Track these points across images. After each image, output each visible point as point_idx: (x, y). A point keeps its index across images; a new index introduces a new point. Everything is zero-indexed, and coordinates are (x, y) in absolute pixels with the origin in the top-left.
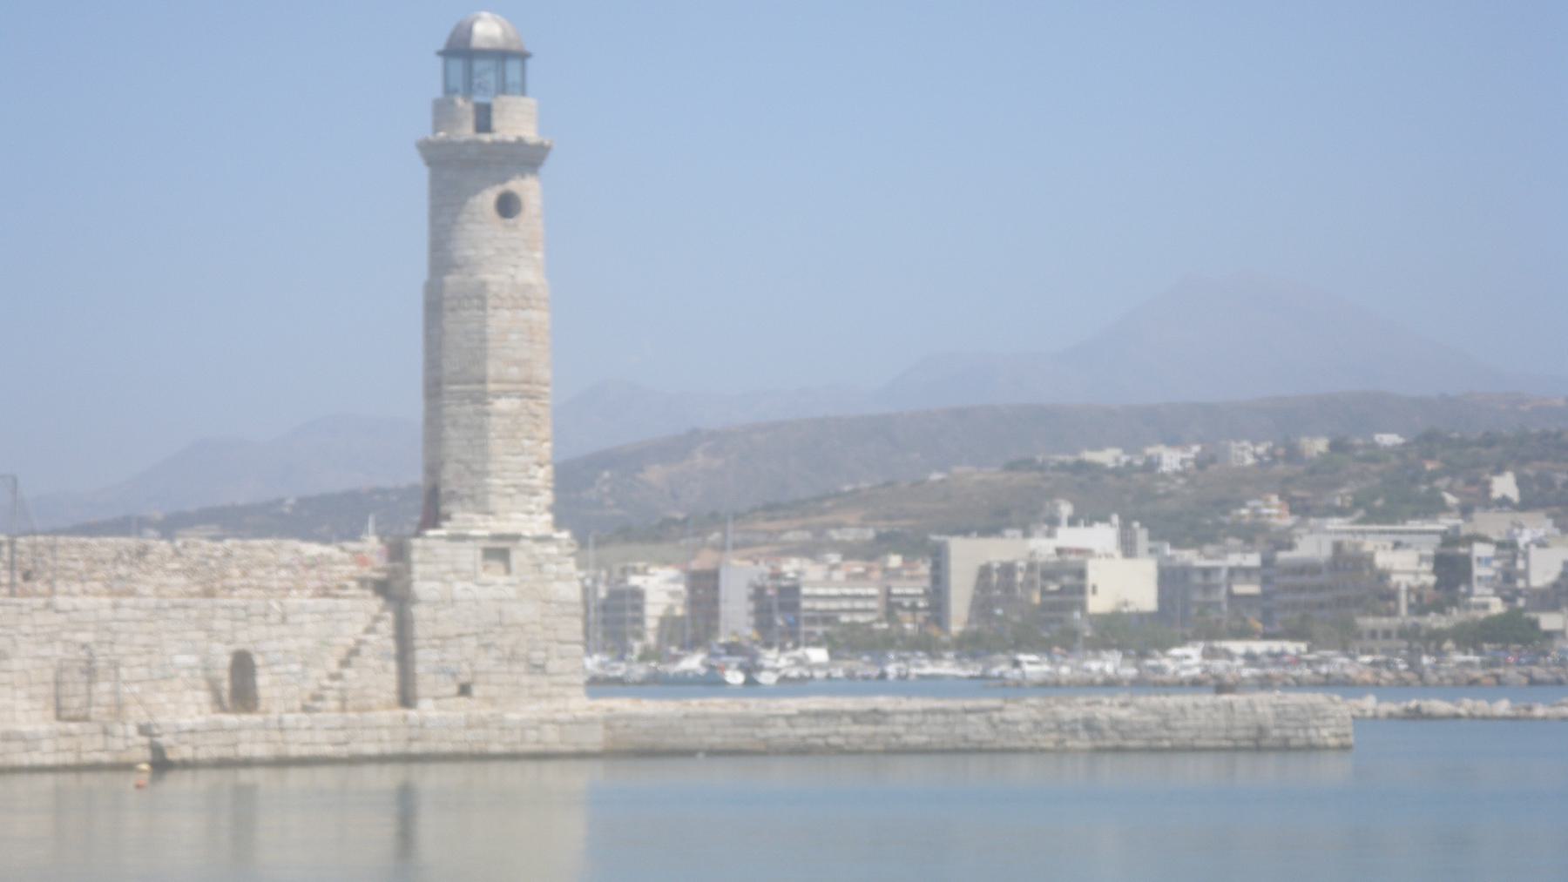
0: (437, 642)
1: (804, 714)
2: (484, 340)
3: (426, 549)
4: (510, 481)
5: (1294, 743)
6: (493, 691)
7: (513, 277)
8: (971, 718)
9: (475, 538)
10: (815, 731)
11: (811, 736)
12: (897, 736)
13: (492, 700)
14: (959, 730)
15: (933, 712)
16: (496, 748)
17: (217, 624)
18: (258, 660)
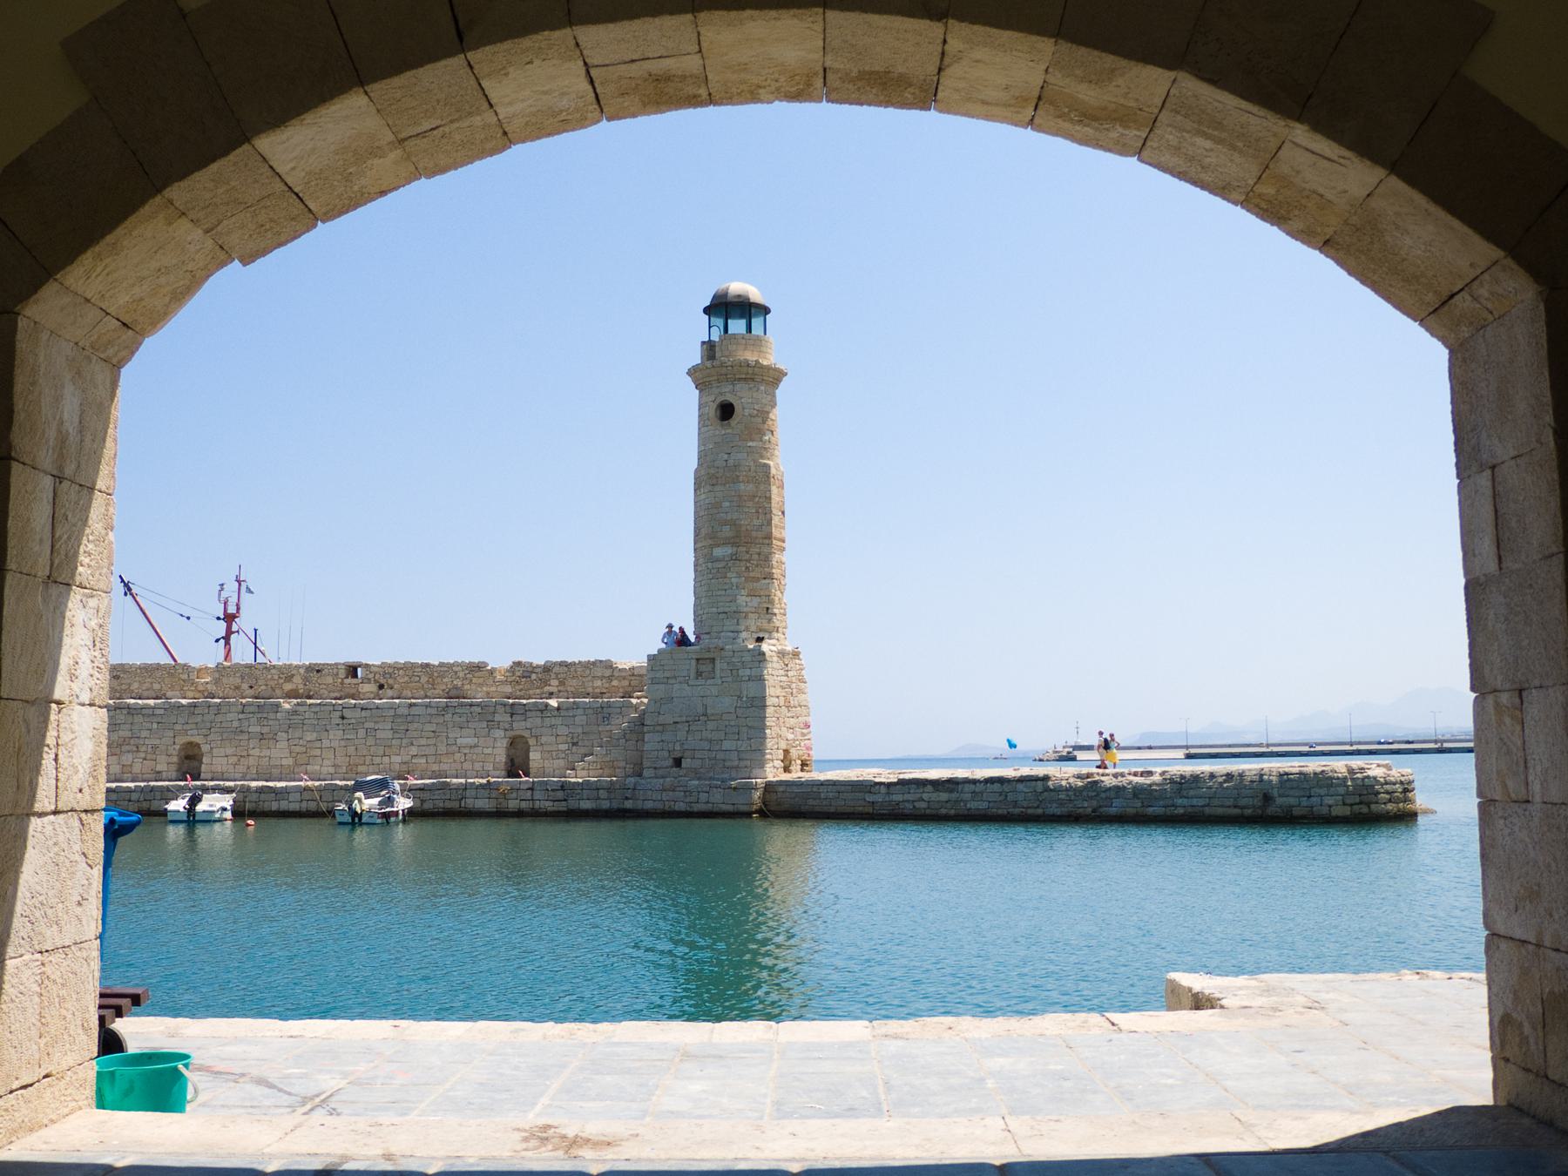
0: (660, 728)
4: (721, 610)
5: (1296, 812)
6: (697, 763)
7: (726, 461)
10: (907, 797)
14: (1011, 797)
17: (497, 718)
18: (532, 742)
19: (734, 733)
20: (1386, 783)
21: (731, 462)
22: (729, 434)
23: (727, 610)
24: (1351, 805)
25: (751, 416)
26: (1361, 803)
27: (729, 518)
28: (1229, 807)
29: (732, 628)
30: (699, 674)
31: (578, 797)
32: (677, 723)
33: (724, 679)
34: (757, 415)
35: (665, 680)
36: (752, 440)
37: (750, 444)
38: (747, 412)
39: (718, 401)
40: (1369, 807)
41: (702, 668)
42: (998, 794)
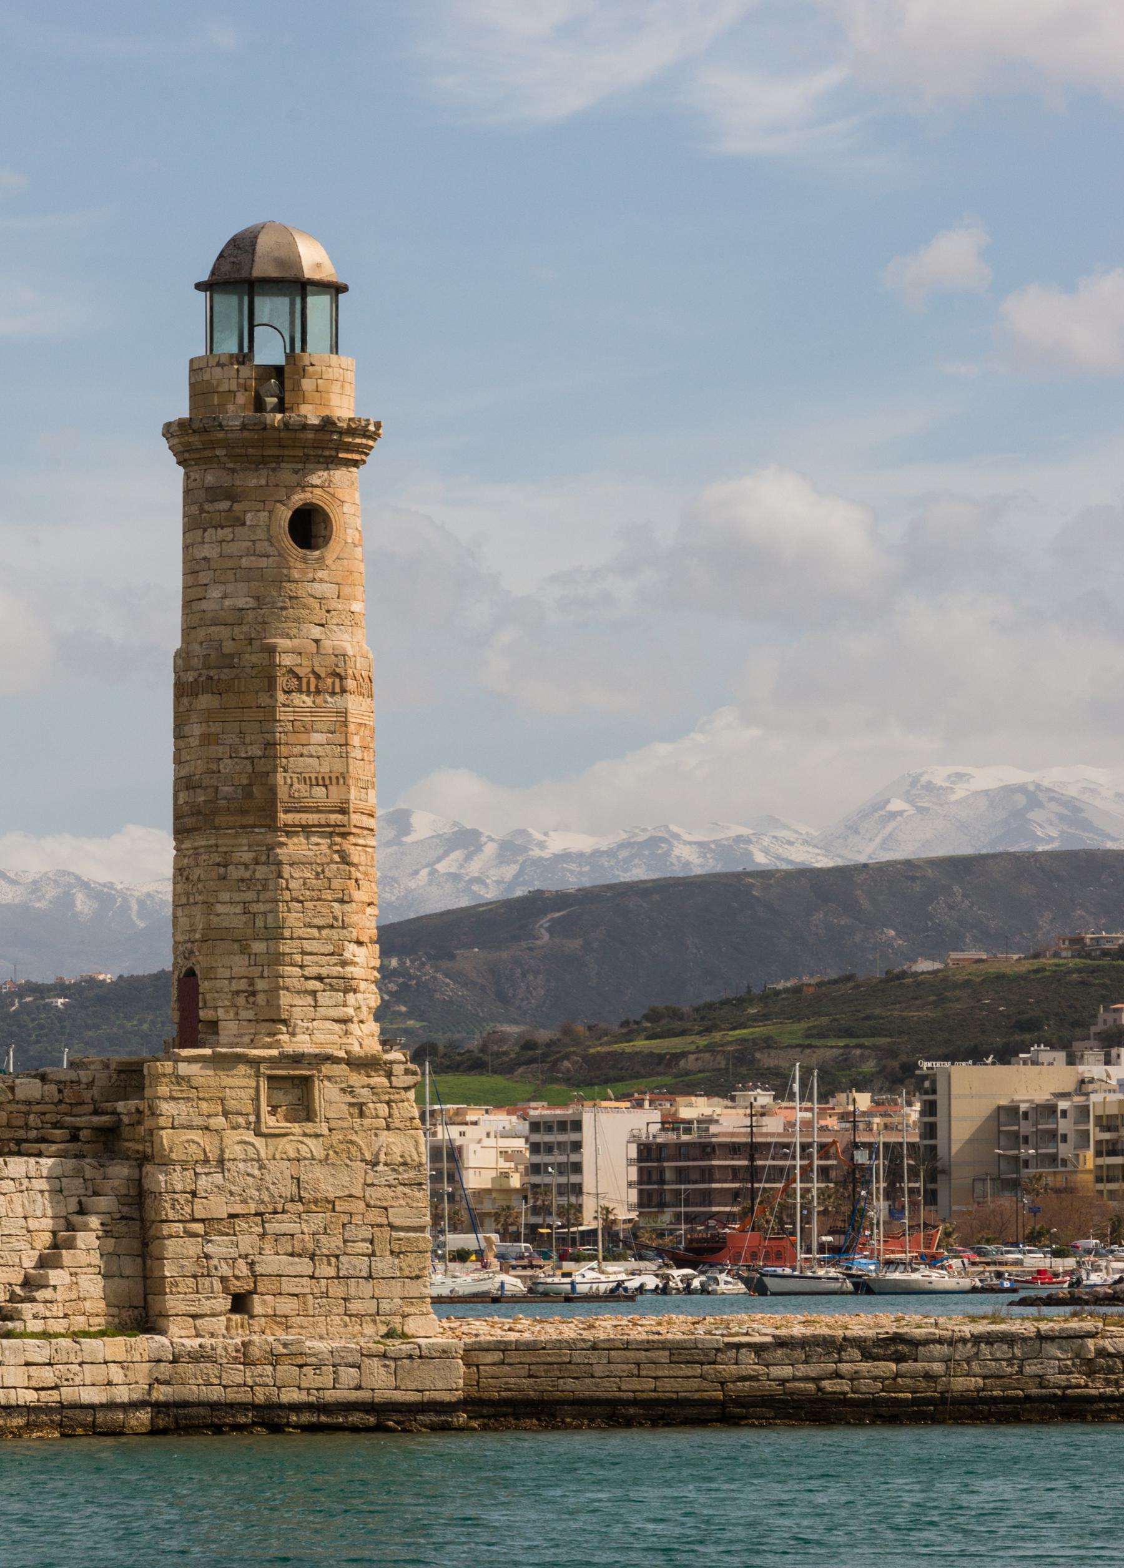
0: (199, 1228)
1: (781, 1343)
2: (271, 745)
3: (179, 1079)
4: (308, 972)
6: (287, 1306)
7: (317, 641)
8: (1053, 1350)
9: (254, 1062)
10: (802, 1370)
11: (795, 1379)
12: (928, 1376)
13: (279, 1319)
15: (989, 1339)
19: (363, 1240)
21: (327, 644)
23: (324, 971)
27: (325, 769)
31: (78, 1381)
32: (236, 1216)
42: (1004, 1363)
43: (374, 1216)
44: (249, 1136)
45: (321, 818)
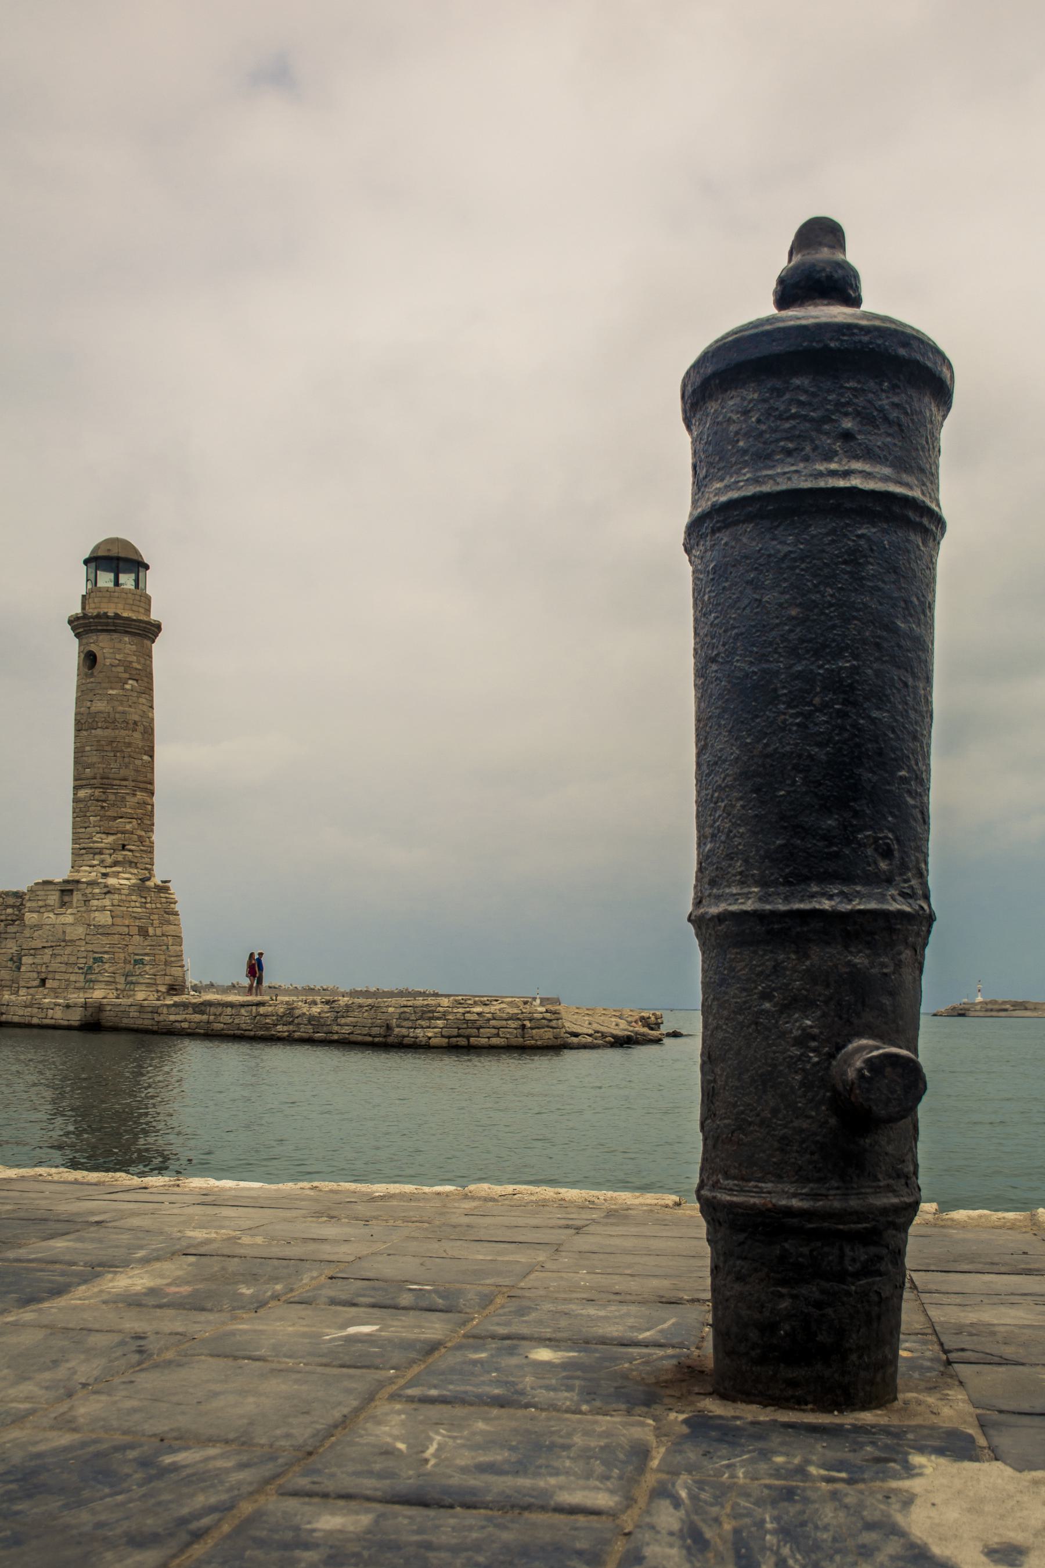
0: (32, 952)
5: (406, 1041)
7: (89, 708)
16: (35, 1021)
20: (494, 1019)
22: (92, 682)
24: (449, 1037)
25: (113, 666)
26: (458, 1036)
28: (365, 1035)
29: (89, 863)
30: (63, 904)
33: (79, 909)
34: (118, 665)
35: (37, 909)
36: (112, 688)
37: (111, 692)
38: (108, 662)
39: (85, 651)
40: (469, 1041)
41: (66, 899)
43: (90, 948)
44: (51, 915)
45: (87, 782)
